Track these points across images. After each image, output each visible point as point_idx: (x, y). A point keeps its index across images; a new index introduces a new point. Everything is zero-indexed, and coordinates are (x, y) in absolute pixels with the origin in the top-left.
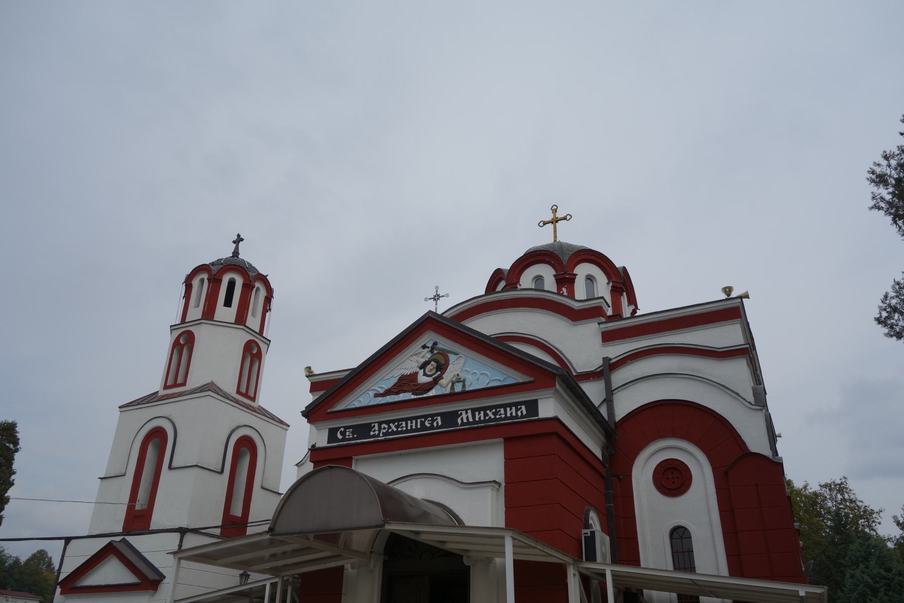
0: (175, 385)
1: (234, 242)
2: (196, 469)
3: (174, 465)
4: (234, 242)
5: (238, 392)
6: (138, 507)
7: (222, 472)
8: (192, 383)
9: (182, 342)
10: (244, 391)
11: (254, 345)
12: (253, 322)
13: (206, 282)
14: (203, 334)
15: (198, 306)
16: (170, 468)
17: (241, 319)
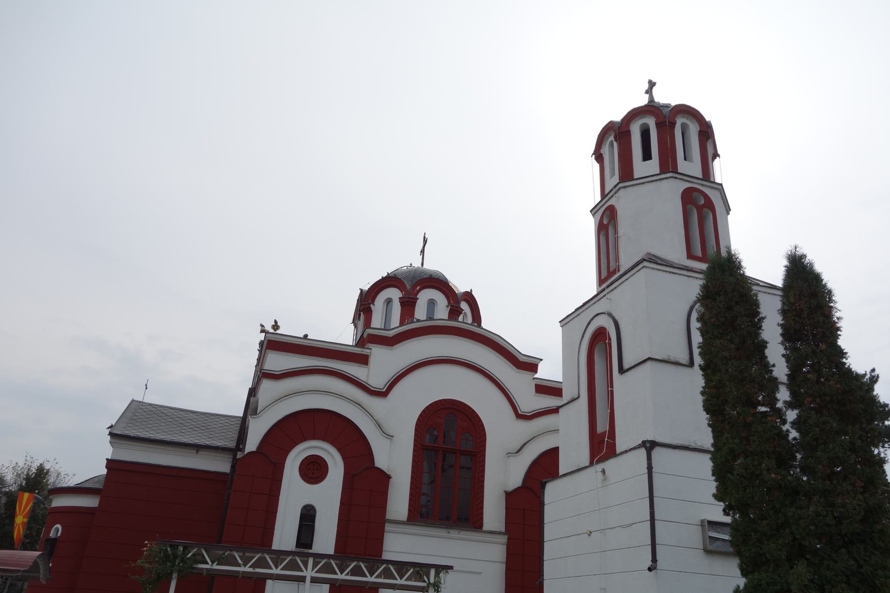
0: (610, 274)
1: (647, 92)
2: (649, 363)
3: (626, 366)
4: (647, 92)
5: (690, 256)
6: (600, 430)
7: (691, 364)
8: (625, 263)
9: (605, 222)
10: (700, 254)
11: (695, 194)
12: (691, 167)
13: (615, 144)
14: (624, 202)
15: (614, 174)
16: (622, 371)
17: (668, 165)
